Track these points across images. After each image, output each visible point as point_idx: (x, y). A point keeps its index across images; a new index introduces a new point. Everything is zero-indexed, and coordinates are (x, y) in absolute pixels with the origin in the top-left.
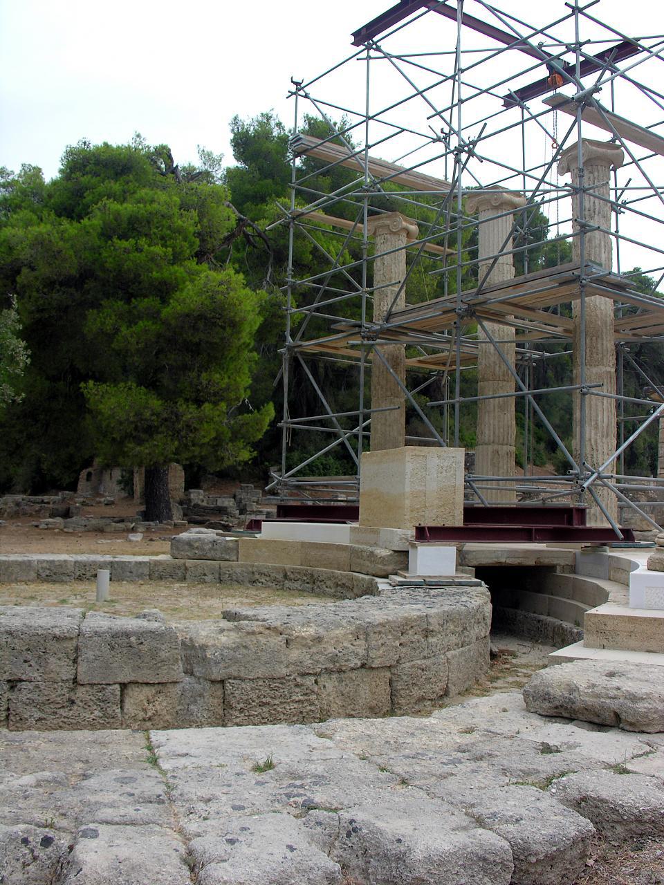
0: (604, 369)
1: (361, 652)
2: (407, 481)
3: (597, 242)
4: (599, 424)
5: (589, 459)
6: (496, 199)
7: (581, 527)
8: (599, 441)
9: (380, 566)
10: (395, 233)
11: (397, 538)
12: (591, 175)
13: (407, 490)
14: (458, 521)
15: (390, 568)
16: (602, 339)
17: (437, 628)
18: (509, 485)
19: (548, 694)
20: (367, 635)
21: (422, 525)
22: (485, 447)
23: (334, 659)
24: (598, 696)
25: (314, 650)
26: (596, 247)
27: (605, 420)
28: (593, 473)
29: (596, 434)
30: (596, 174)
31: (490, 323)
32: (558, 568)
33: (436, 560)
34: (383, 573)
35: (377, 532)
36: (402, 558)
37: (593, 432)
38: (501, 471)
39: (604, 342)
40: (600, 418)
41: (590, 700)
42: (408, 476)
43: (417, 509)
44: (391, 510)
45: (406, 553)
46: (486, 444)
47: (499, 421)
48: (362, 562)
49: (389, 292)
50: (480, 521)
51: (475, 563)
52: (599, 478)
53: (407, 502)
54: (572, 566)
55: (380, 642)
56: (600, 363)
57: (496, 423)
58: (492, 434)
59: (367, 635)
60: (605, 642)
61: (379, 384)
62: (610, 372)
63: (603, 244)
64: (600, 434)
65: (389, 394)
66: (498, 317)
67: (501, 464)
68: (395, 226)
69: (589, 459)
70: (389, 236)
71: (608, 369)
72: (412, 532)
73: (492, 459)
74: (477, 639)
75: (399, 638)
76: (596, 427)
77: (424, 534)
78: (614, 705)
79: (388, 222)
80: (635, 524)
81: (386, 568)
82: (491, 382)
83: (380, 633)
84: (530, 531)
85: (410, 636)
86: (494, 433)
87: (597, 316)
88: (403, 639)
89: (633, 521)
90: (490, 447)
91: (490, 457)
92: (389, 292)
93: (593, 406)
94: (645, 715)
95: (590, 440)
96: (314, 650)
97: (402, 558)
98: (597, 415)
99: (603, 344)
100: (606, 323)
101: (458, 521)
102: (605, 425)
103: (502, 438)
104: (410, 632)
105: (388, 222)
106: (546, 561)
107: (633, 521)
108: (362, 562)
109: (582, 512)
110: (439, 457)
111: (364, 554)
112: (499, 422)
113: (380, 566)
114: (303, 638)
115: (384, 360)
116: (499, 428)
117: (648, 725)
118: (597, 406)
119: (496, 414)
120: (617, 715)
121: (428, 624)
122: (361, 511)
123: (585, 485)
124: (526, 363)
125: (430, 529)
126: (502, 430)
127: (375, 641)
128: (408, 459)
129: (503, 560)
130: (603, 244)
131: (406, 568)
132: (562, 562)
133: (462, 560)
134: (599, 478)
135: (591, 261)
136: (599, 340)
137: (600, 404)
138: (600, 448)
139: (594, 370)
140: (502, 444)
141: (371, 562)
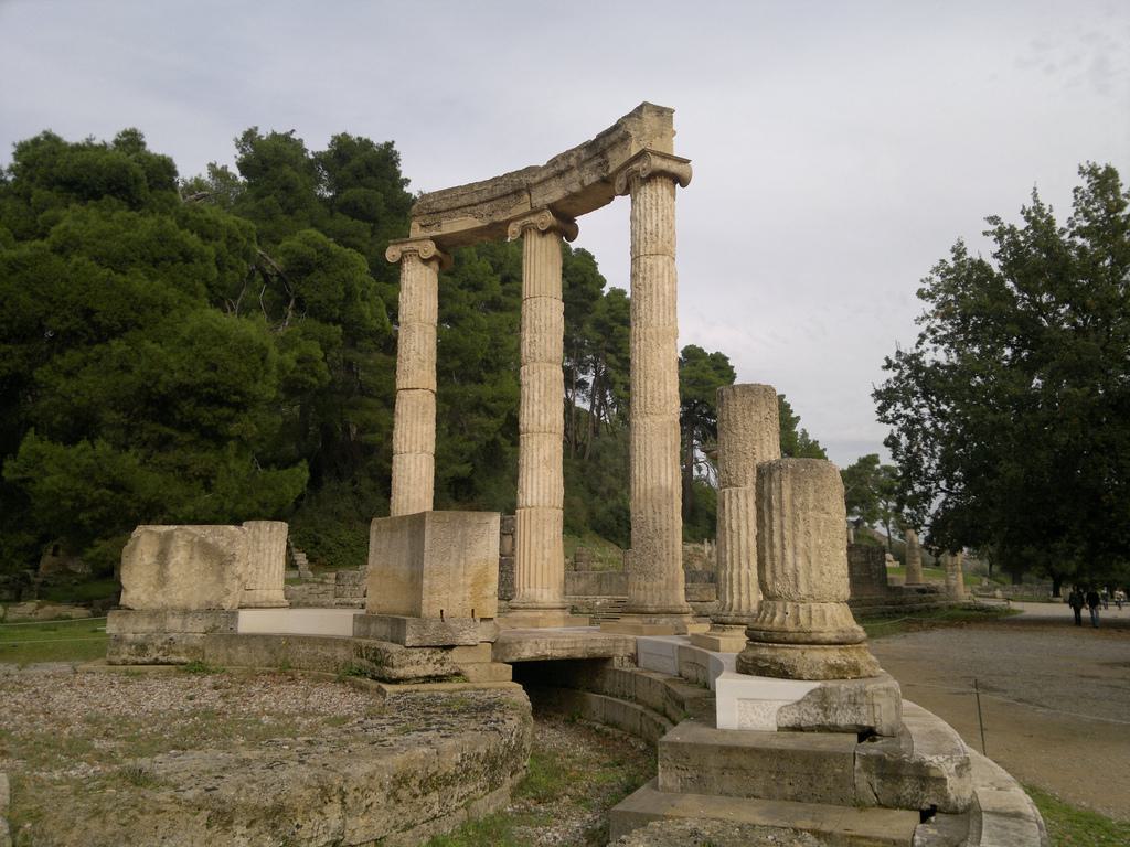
3: (660, 271)
5: (651, 524)
6: (542, 223)
16: (665, 384)
26: (658, 277)
40: (663, 475)
58: (535, 495)
63: (666, 274)
69: (651, 524)
93: (656, 461)
98: (659, 471)
116: (544, 487)
118: (659, 461)
119: (541, 471)
126: (547, 490)
130: (666, 274)
137: (663, 459)
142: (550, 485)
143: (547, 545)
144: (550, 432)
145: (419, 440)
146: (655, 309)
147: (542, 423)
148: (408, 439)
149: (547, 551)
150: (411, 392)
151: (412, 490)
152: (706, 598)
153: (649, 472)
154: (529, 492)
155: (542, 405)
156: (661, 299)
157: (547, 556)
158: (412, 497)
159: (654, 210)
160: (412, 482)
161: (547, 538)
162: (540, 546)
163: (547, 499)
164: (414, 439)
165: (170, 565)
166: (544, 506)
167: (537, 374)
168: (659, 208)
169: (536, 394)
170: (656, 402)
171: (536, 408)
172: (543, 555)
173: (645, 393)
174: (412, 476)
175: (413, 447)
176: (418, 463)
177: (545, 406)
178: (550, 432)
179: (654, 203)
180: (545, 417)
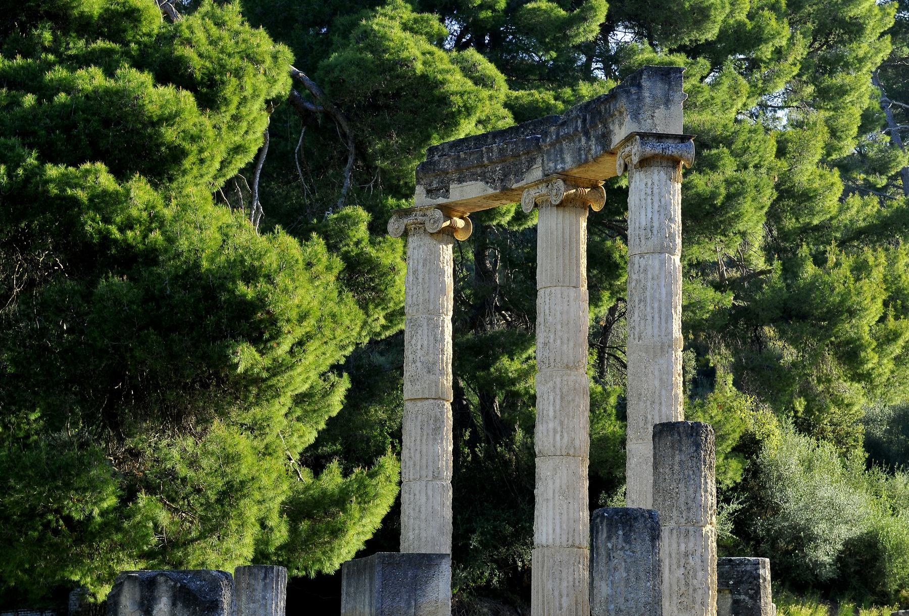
58: (551, 531)
126: (564, 526)
142: (568, 519)
143: (565, 592)
144: (568, 455)
145: (431, 464)
146: (649, 318)
147: (558, 445)
148: (418, 463)
149: (564, 599)
150: (419, 404)
151: (423, 525)
154: (544, 530)
155: (557, 421)
157: (565, 605)
158: (424, 534)
159: (649, 201)
160: (423, 517)
161: (565, 584)
162: (556, 593)
163: (564, 538)
164: (424, 461)
165: (155, 612)
166: (561, 546)
167: (551, 384)
168: (656, 199)
169: (551, 408)
171: (551, 425)
172: (560, 604)
174: (423, 509)
175: (424, 473)
176: (430, 493)
177: (562, 423)
178: (568, 455)
180: (562, 437)
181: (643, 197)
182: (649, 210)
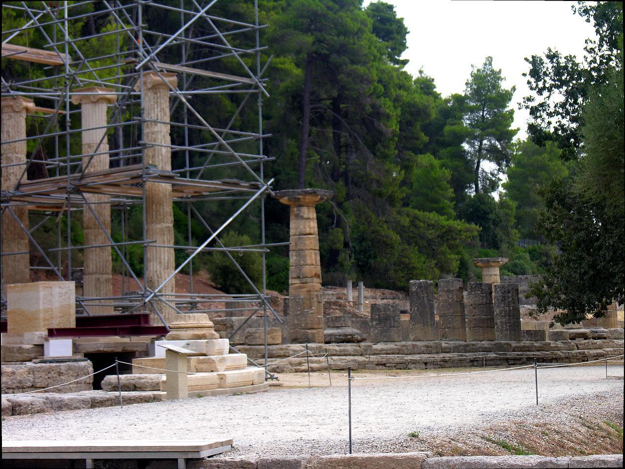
0: (164, 225)
1: (32, 379)
2: (41, 303)
4: (162, 260)
7: (146, 325)
8: (162, 272)
9: (26, 355)
10: (17, 112)
11: (36, 337)
12: (155, 96)
13: (41, 307)
14: (73, 325)
15: (33, 355)
16: (163, 205)
17: (64, 372)
18: (108, 303)
19: (110, 382)
20: (33, 372)
21: (51, 328)
22: (90, 276)
23: (20, 382)
24: (128, 380)
25: (12, 378)
27: (166, 258)
28: (152, 293)
29: (160, 267)
30: (159, 94)
31: (91, 195)
32: (137, 353)
33: (61, 347)
34: (29, 359)
35: (21, 335)
36: (40, 348)
37: (158, 266)
38: (102, 293)
39: (165, 208)
40: (162, 256)
41: (125, 382)
42: (41, 299)
43: (48, 319)
44: (30, 321)
45: (42, 346)
46: (91, 274)
47: (99, 258)
48: (13, 354)
49: (14, 158)
50: (86, 325)
51: (84, 351)
52: (155, 296)
53: (41, 315)
54: (145, 351)
55: (40, 375)
56: (162, 221)
57: (98, 259)
58: (94, 267)
59: (33, 372)
60: (142, 372)
61: (8, 229)
62: (169, 227)
64: (163, 268)
65: (17, 237)
66: (95, 190)
67: (102, 288)
68: (17, 106)
70: (12, 114)
71: (168, 225)
72: (45, 333)
73: (96, 285)
74: (85, 382)
75: (47, 375)
76: (160, 263)
77: (54, 333)
78: (133, 382)
79: (11, 103)
80: (260, 337)
81: (30, 355)
82: (93, 230)
83: (39, 371)
84: (116, 329)
85: (52, 374)
86: (96, 266)
87: (159, 190)
88: (49, 376)
89: (257, 335)
90: (94, 277)
91: (94, 283)
92: (14, 158)
94: (144, 384)
95: (156, 271)
96: (12, 378)
97: (40, 349)
98: (161, 255)
99: (163, 209)
100: (166, 195)
101: (73, 325)
102: (166, 261)
103: (101, 270)
104: (52, 372)
105: (11, 103)
106: (129, 349)
107: (257, 335)
108: (13, 354)
109: (146, 317)
110: (60, 287)
111: (15, 350)
112: (100, 256)
113: (26, 355)
114: (7, 372)
115: (13, 212)
116: (100, 262)
117: (146, 388)
120: (135, 386)
121: (60, 369)
122: (9, 323)
123: (147, 300)
124: (122, 208)
125: (57, 330)
126: (101, 264)
127: (37, 375)
128: (41, 289)
129: (101, 349)
131: (43, 354)
132: (140, 349)
133: (76, 348)
134: (155, 296)
135: (149, 164)
136: (161, 207)
138: (163, 276)
139: (158, 226)
140: (102, 274)
141: (20, 353)
152: (270, 341)
153: (155, 255)
156: (160, 157)
159: (156, 106)
170: (158, 216)
173: (152, 212)
179: (155, 101)
181: (152, 103)
182: (156, 109)
